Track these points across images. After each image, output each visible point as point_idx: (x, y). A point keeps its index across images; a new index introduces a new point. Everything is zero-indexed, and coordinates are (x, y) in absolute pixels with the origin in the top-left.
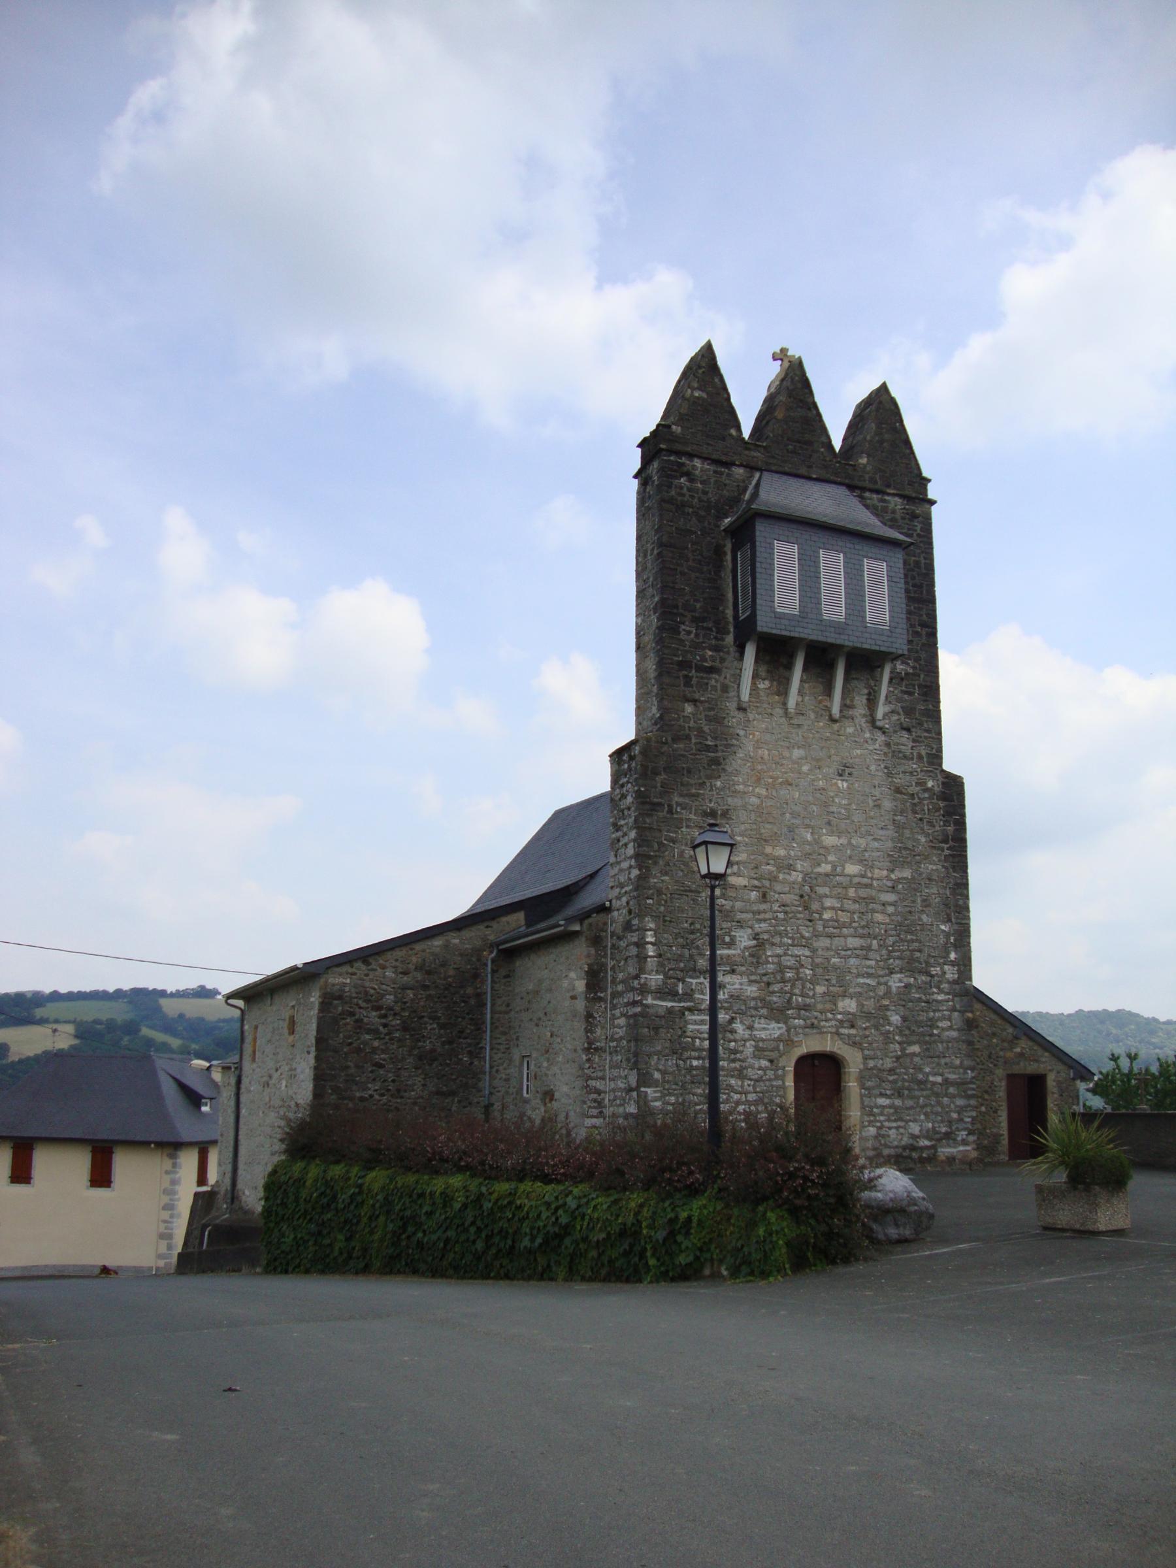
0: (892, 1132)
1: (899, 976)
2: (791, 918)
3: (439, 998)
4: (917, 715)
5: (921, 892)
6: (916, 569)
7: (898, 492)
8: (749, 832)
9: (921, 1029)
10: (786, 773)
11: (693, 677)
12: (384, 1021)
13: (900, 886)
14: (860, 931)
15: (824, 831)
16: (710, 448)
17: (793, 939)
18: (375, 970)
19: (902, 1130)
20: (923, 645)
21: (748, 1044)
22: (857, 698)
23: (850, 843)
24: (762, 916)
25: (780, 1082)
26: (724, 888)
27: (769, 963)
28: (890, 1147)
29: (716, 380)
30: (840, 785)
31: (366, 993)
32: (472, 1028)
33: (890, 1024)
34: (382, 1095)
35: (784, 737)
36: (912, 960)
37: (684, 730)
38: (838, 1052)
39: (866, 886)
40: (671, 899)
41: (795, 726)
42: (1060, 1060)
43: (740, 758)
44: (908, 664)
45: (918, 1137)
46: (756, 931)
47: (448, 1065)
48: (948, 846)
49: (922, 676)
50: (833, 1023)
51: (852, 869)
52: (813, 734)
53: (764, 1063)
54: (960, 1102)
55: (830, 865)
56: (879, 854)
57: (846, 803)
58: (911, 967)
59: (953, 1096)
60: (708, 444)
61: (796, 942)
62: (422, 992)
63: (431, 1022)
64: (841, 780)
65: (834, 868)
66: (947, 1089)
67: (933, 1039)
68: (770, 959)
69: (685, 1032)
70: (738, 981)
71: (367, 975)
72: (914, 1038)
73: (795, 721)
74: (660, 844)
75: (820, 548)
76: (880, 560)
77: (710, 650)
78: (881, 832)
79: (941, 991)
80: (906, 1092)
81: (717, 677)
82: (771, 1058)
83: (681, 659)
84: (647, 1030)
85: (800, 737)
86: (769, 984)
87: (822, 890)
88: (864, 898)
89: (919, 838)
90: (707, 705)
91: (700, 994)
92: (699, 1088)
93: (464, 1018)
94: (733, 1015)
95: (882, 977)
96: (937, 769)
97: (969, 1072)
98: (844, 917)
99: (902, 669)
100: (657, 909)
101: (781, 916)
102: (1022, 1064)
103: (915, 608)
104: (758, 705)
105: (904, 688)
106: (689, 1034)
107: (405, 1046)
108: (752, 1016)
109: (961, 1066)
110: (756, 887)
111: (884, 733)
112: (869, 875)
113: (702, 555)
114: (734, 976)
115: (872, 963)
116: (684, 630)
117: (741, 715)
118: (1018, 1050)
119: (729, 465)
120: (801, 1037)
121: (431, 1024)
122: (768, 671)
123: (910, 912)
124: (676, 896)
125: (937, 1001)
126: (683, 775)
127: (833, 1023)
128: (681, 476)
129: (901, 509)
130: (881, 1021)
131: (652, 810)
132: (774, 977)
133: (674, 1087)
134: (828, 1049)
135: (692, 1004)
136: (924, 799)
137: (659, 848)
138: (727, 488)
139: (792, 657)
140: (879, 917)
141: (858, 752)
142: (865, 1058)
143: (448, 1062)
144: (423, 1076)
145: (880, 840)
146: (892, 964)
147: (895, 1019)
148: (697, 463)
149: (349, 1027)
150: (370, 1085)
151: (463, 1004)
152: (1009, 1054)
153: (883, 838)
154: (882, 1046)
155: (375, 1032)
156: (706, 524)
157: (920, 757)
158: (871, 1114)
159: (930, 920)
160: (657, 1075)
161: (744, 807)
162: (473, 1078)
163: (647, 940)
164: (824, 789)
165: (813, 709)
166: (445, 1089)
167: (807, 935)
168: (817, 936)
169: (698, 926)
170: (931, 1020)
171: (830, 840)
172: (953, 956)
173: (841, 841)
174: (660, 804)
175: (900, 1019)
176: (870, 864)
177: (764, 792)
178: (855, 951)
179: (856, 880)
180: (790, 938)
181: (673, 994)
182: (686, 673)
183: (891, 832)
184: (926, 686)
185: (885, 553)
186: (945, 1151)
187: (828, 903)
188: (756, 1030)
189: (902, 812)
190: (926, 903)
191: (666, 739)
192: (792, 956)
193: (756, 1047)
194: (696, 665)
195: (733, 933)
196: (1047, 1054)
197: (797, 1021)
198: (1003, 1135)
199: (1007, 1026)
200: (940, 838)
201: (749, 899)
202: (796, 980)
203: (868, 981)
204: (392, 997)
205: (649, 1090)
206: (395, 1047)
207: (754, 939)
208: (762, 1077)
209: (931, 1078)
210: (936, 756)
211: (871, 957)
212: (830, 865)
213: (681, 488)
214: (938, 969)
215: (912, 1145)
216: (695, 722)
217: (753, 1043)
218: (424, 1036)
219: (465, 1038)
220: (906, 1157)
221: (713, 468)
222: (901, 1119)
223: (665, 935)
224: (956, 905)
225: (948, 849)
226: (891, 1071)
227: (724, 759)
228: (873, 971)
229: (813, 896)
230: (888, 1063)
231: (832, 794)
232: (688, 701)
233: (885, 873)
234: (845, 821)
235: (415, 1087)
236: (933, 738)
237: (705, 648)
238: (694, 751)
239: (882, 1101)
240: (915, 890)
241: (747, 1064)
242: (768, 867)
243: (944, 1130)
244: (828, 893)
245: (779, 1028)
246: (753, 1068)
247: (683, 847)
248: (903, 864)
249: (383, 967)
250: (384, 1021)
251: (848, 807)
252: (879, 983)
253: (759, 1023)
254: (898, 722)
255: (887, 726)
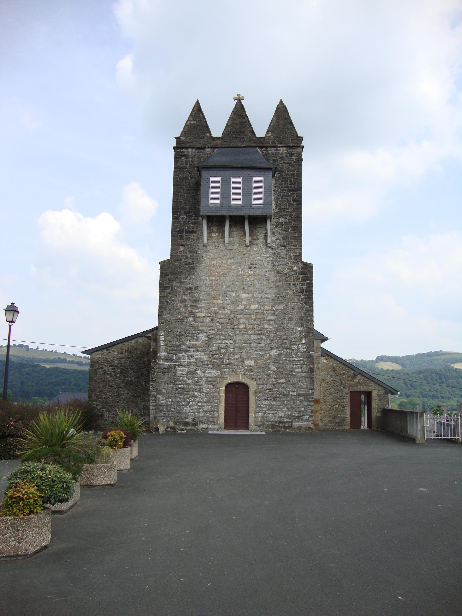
0: (270, 415)
1: (276, 350)
2: (224, 328)
3: (134, 362)
4: (290, 239)
5: (288, 314)
6: (292, 177)
7: (286, 145)
8: (206, 295)
9: (286, 372)
10: (224, 270)
11: (184, 236)
12: (114, 370)
13: (278, 313)
14: (257, 332)
15: (241, 292)
16: (197, 143)
17: (225, 336)
18: (111, 352)
19: (275, 415)
20: (294, 209)
21: (203, 379)
22: (259, 235)
23: (253, 296)
24: (211, 328)
25: (217, 394)
26: (194, 318)
27: (214, 347)
28: (269, 421)
29: (201, 115)
30: (250, 273)
31: (107, 361)
32: (146, 372)
33: (270, 370)
34: (112, 397)
35: (224, 255)
36: (282, 343)
37: (179, 257)
38: (245, 382)
39: (261, 313)
40: (171, 323)
41: (230, 250)
42: (379, 385)
43: (203, 266)
44: (286, 218)
45: (283, 417)
46: (208, 334)
47: (137, 386)
48: (303, 294)
49: (293, 222)
50: (243, 370)
51: (254, 307)
52: (238, 252)
53: (210, 386)
54: (305, 403)
55: (243, 306)
56: (267, 300)
57: (252, 279)
58: (282, 346)
59: (302, 401)
60: (196, 142)
61: (226, 338)
62: (128, 360)
63: (131, 370)
64: (250, 270)
65: (245, 307)
66: (299, 398)
67: (292, 376)
68: (214, 345)
69: (176, 374)
70: (199, 354)
71: (108, 354)
72: (283, 376)
73: (229, 248)
74: (167, 302)
75: (231, 177)
76: (260, 177)
77: (192, 224)
78: (269, 291)
79: (298, 356)
80: (278, 399)
81: (194, 234)
82: (213, 384)
83: (179, 229)
84: (160, 373)
85: (232, 254)
86: (213, 355)
87: (239, 316)
88: (260, 319)
89: (288, 291)
90: (189, 246)
91: (182, 359)
92: (181, 396)
93: (143, 369)
94: (197, 367)
95: (267, 351)
96: (299, 262)
97: (311, 390)
98: (249, 327)
99: (283, 221)
100: (166, 327)
101: (220, 327)
102: (359, 387)
103: (290, 194)
104: (213, 243)
105: (283, 229)
106: (177, 375)
107: (121, 379)
108: (205, 368)
109: (306, 388)
110: (209, 316)
111: (272, 249)
112: (262, 309)
113: (190, 187)
114: (198, 352)
115: (263, 345)
116: (181, 218)
117: (204, 248)
118: (357, 381)
119: (204, 148)
120: (227, 376)
121: (131, 371)
122: (218, 229)
123: (282, 323)
124: (174, 322)
125: (295, 360)
126: (178, 275)
127: (243, 370)
128: (182, 157)
129: (286, 152)
130: (266, 369)
131: (164, 290)
132: (216, 352)
133: (171, 395)
134: (240, 381)
135: (179, 363)
136: (291, 275)
137: (167, 304)
138: (203, 158)
139: (224, 222)
140: (267, 326)
141: (259, 258)
142: (258, 385)
143: (137, 385)
144: (127, 390)
145: (268, 294)
146: (273, 345)
147: (273, 368)
148: (190, 150)
149: (101, 373)
150: (108, 394)
151: (143, 364)
152: (352, 383)
153: (269, 293)
154: (266, 379)
155: (110, 374)
156: (192, 174)
157: (290, 257)
158: (260, 407)
159: (292, 326)
160: (164, 391)
161: (205, 285)
162: (146, 391)
163: (161, 339)
164: (242, 275)
165: (238, 243)
166: (135, 395)
167: (232, 335)
168: (236, 335)
169: (182, 333)
170: (291, 368)
171: (243, 296)
172: (304, 341)
173: (249, 296)
174: (168, 287)
175: (275, 368)
176: (263, 304)
177: (214, 278)
178: (254, 341)
179: (256, 311)
180: (224, 336)
181: (171, 360)
182: (180, 234)
183: (274, 290)
184: (295, 227)
185: (263, 174)
186: (297, 424)
187: (242, 321)
188: (207, 373)
189: (280, 281)
190: (291, 319)
191: (171, 261)
192: (224, 343)
193: (207, 380)
194: (185, 230)
195: (198, 335)
196: (372, 383)
197: (225, 369)
198: (347, 417)
199: (351, 370)
200: (299, 291)
201: (206, 322)
202: (226, 353)
203: (260, 353)
204: (117, 362)
205: (160, 396)
206: (117, 380)
207: (207, 337)
208: (209, 392)
209: (291, 393)
210: (299, 256)
211: (262, 343)
212: (243, 306)
213: (182, 161)
214: (296, 347)
215: (280, 421)
216: (184, 253)
217: (206, 378)
218: (128, 376)
219: (144, 376)
220: (277, 426)
221: (197, 151)
222: (275, 410)
223: (168, 337)
224: (306, 319)
225: (303, 296)
226: (270, 390)
227: (196, 267)
228: (263, 348)
229: (235, 319)
230: (269, 387)
231: (246, 277)
232: (181, 245)
233: (270, 307)
234: (251, 287)
235: (124, 394)
236: (297, 248)
237: (190, 224)
238: (183, 265)
239: (265, 402)
240: (285, 314)
241: (203, 387)
242: (214, 308)
243: (297, 415)
244: (242, 317)
245: (217, 372)
246: (205, 388)
247: (177, 303)
248: (280, 303)
249: (114, 351)
250: (114, 370)
251: (253, 281)
252: (266, 354)
253: (208, 370)
254: (280, 244)
255: (274, 246)
